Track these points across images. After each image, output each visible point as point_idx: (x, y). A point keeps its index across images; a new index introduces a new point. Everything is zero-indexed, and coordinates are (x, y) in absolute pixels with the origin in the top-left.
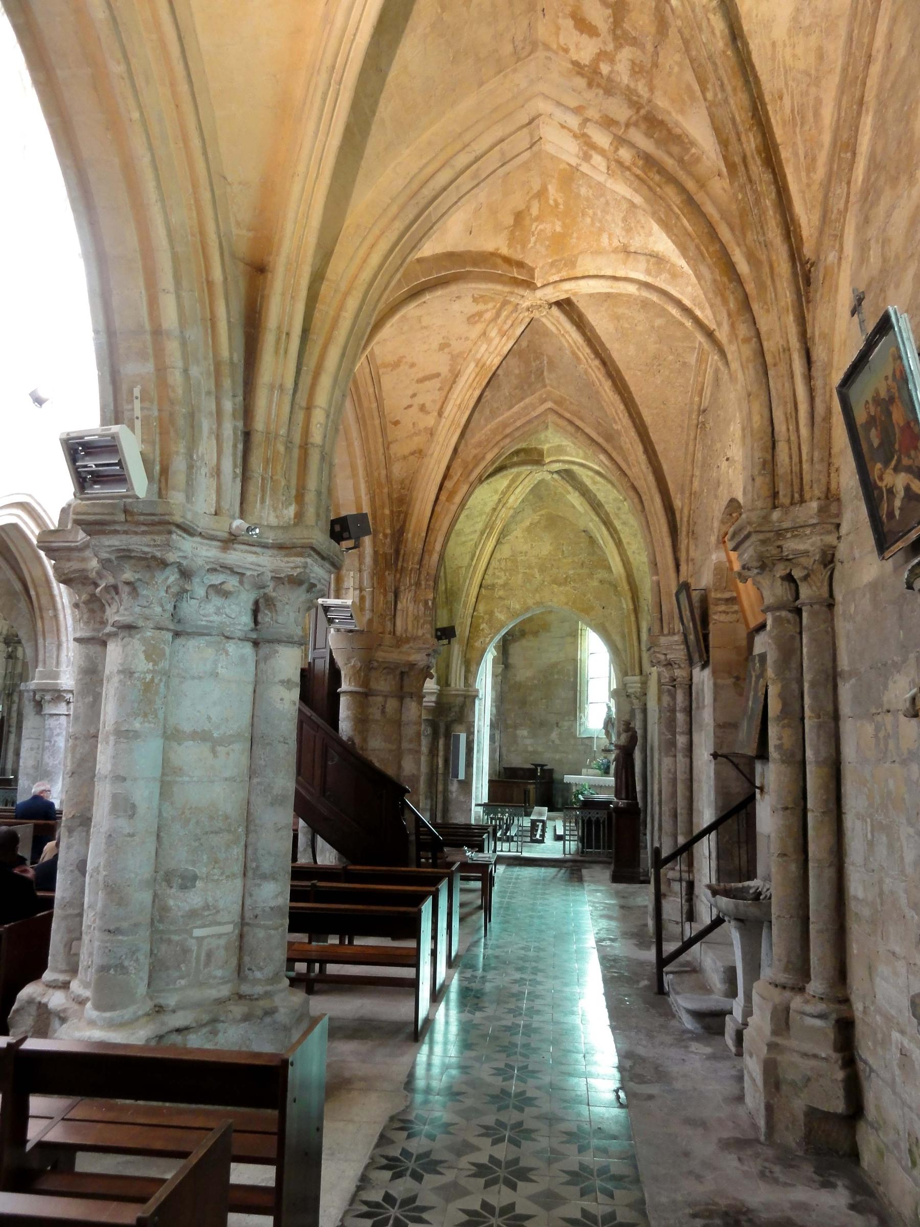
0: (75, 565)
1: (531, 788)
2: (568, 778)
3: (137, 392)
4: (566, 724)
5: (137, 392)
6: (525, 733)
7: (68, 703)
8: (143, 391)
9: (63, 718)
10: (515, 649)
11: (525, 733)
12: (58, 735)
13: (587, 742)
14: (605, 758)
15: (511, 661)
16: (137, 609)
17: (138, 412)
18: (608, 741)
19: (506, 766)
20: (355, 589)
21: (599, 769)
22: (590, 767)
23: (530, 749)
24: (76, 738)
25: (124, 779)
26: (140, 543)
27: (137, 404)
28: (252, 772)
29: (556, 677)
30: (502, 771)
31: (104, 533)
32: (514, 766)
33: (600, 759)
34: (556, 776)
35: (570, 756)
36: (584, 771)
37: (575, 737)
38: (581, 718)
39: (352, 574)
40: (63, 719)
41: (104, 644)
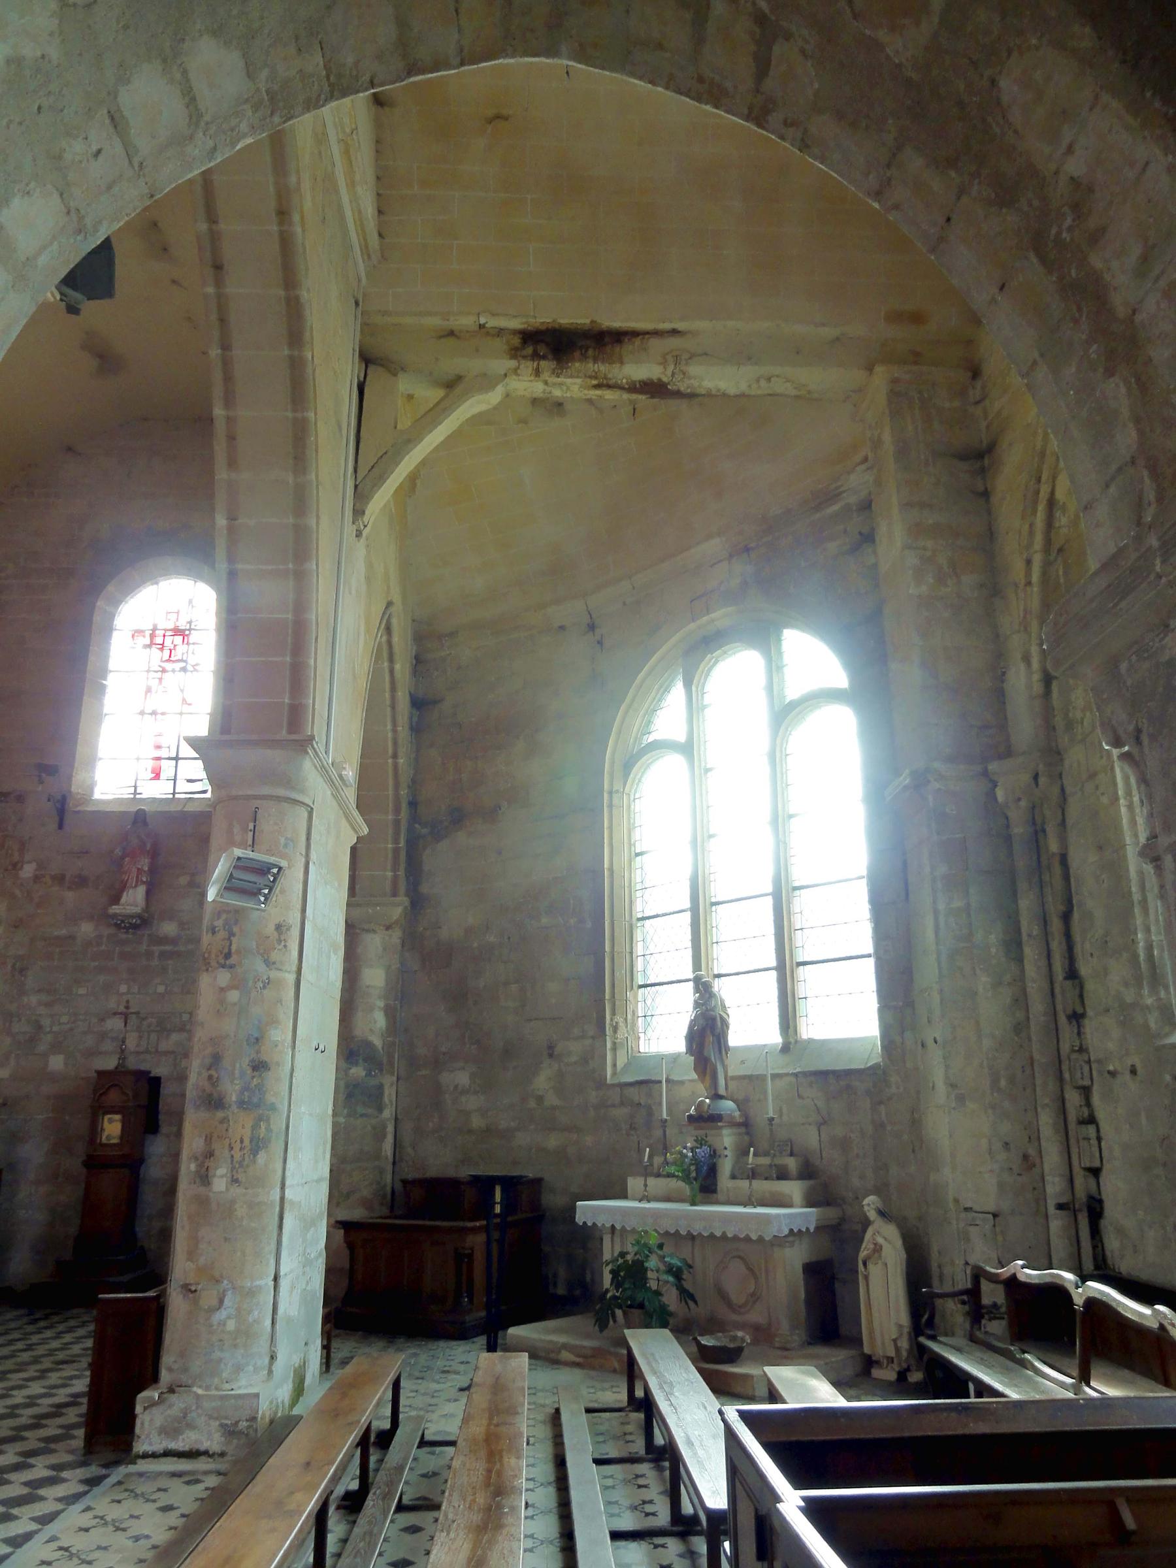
1: (477, 1242)
2: (589, 1211)
4: (575, 1049)
6: (462, 1078)
10: (439, 859)
11: (462, 1078)
13: (634, 1094)
14: (701, 1142)
15: (424, 889)
18: (701, 1088)
19: (412, 1175)
21: (686, 1178)
22: (647, 1172)
23: (477, 1122)
29: (545, 921)
30: (399, 1186)
32: (432, 1172)
33: (685, 1145)
34: (552, 1200)
35: (589, 1140)
36: (634, 1184)
37: (601, 1084)
38: (615, 1029)
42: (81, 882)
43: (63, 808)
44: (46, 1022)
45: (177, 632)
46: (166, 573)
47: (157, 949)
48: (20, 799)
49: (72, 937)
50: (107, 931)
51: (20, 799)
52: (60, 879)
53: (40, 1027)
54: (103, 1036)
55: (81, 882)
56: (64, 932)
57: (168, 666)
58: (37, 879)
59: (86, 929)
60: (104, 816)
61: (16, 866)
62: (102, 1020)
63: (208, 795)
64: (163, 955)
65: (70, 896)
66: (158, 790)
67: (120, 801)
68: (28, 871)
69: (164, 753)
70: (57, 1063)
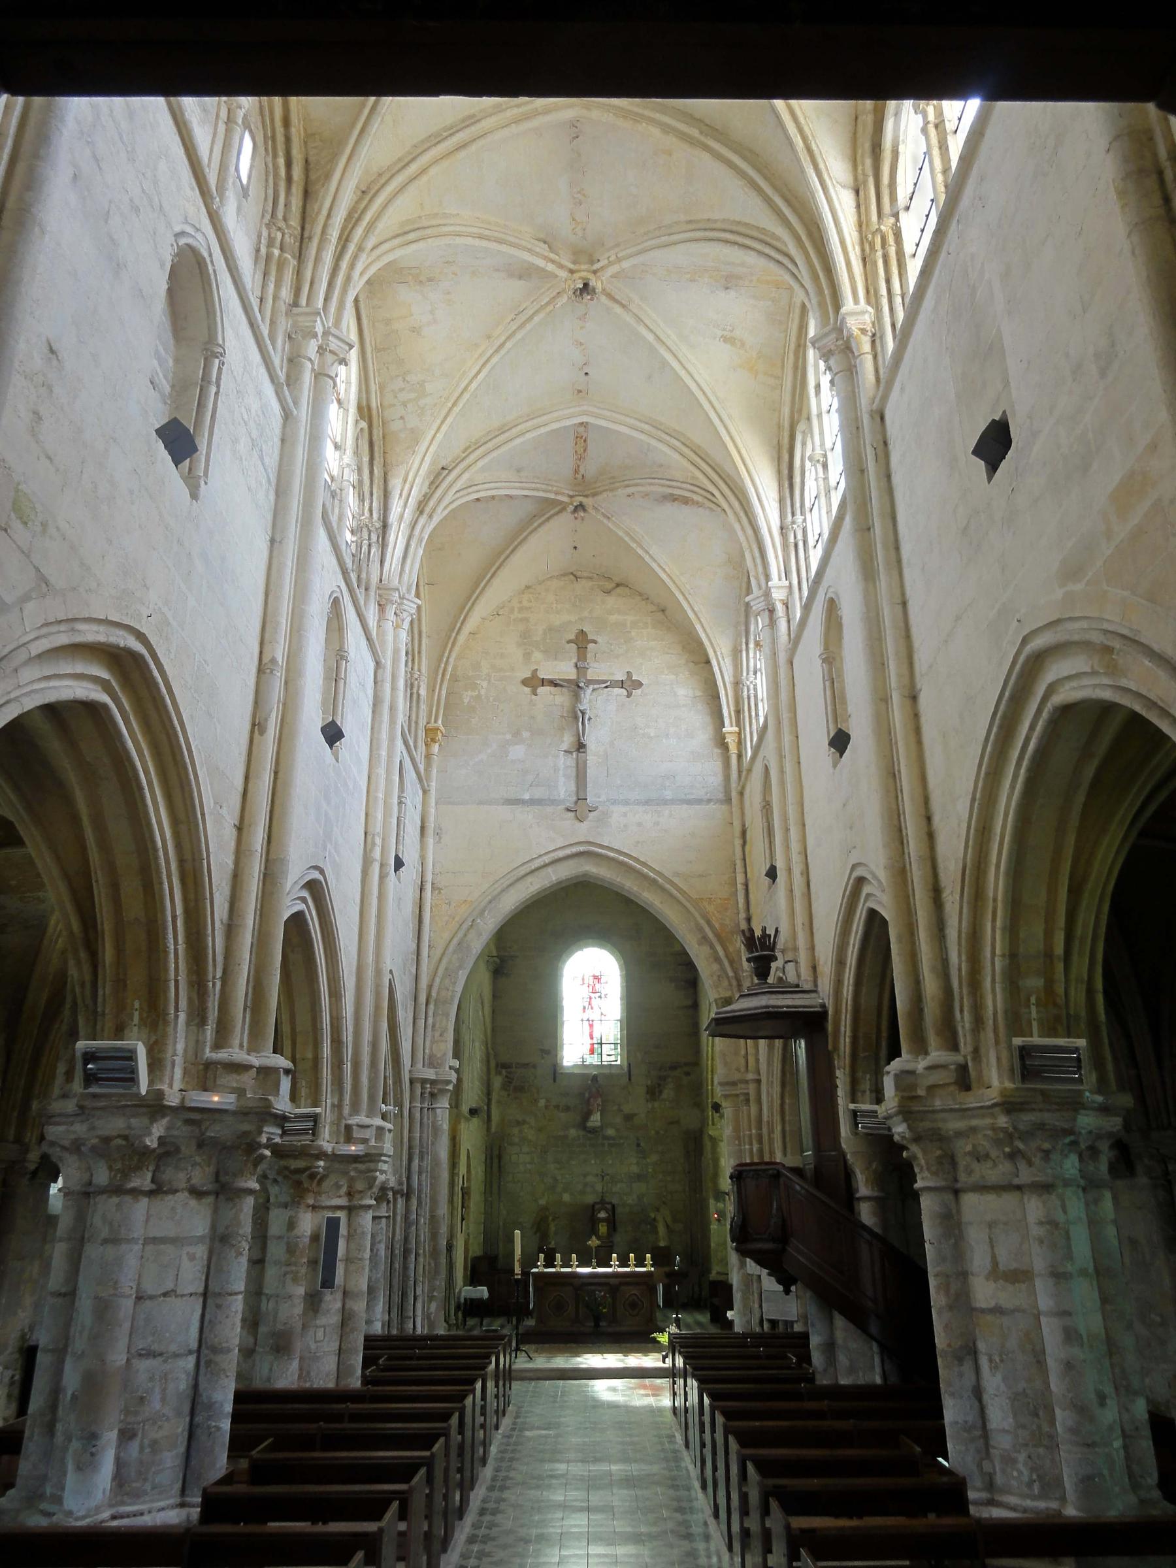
0: (927, 1124)
3: (1033, 1000)
5: (1033, 1000)
7: (388, 1202)
8: (1038, 999)
9: (384, 1220)
12: (380, 1242)
16: (1049, 1171)
17: (1034, 1014)
20: (871, 1091)
24: (947, 1276)
25: (1070, 1314)
26: (1052, 1119)
27: (1034, 1009)
28: (1104, 1300)
31: (1021, 1110)
39: (868, 1076)
40: (384, 1220)
41: (956, 1193)
42: (567, 1109)
43: (555, 1070)
44: (559, 1178)
45: (595, 977)
46: (587, 946)
47: (606, 1142)
48: (534, 1067)
49: (566, 1137)
50: (582, 1133)
51: (534, 1067)
52: (557, 1107)
53: (556, 1180)
54: (586, 1185)
55: (567, 1109)
56: (561, 1133)
57: (593, 995)
58: (546, 1107)
59: (573, 1132)
60: (570, 1076)
61: (536, 1101)
62: (585, 1176)
63: (618, 1063)
64: (611, 1145)
65: (562, 1115)
66: (593, 1060)
67: (575, 1066)
68: (542, 1103)
69: (595, 1041)
70: (566, 1197)
